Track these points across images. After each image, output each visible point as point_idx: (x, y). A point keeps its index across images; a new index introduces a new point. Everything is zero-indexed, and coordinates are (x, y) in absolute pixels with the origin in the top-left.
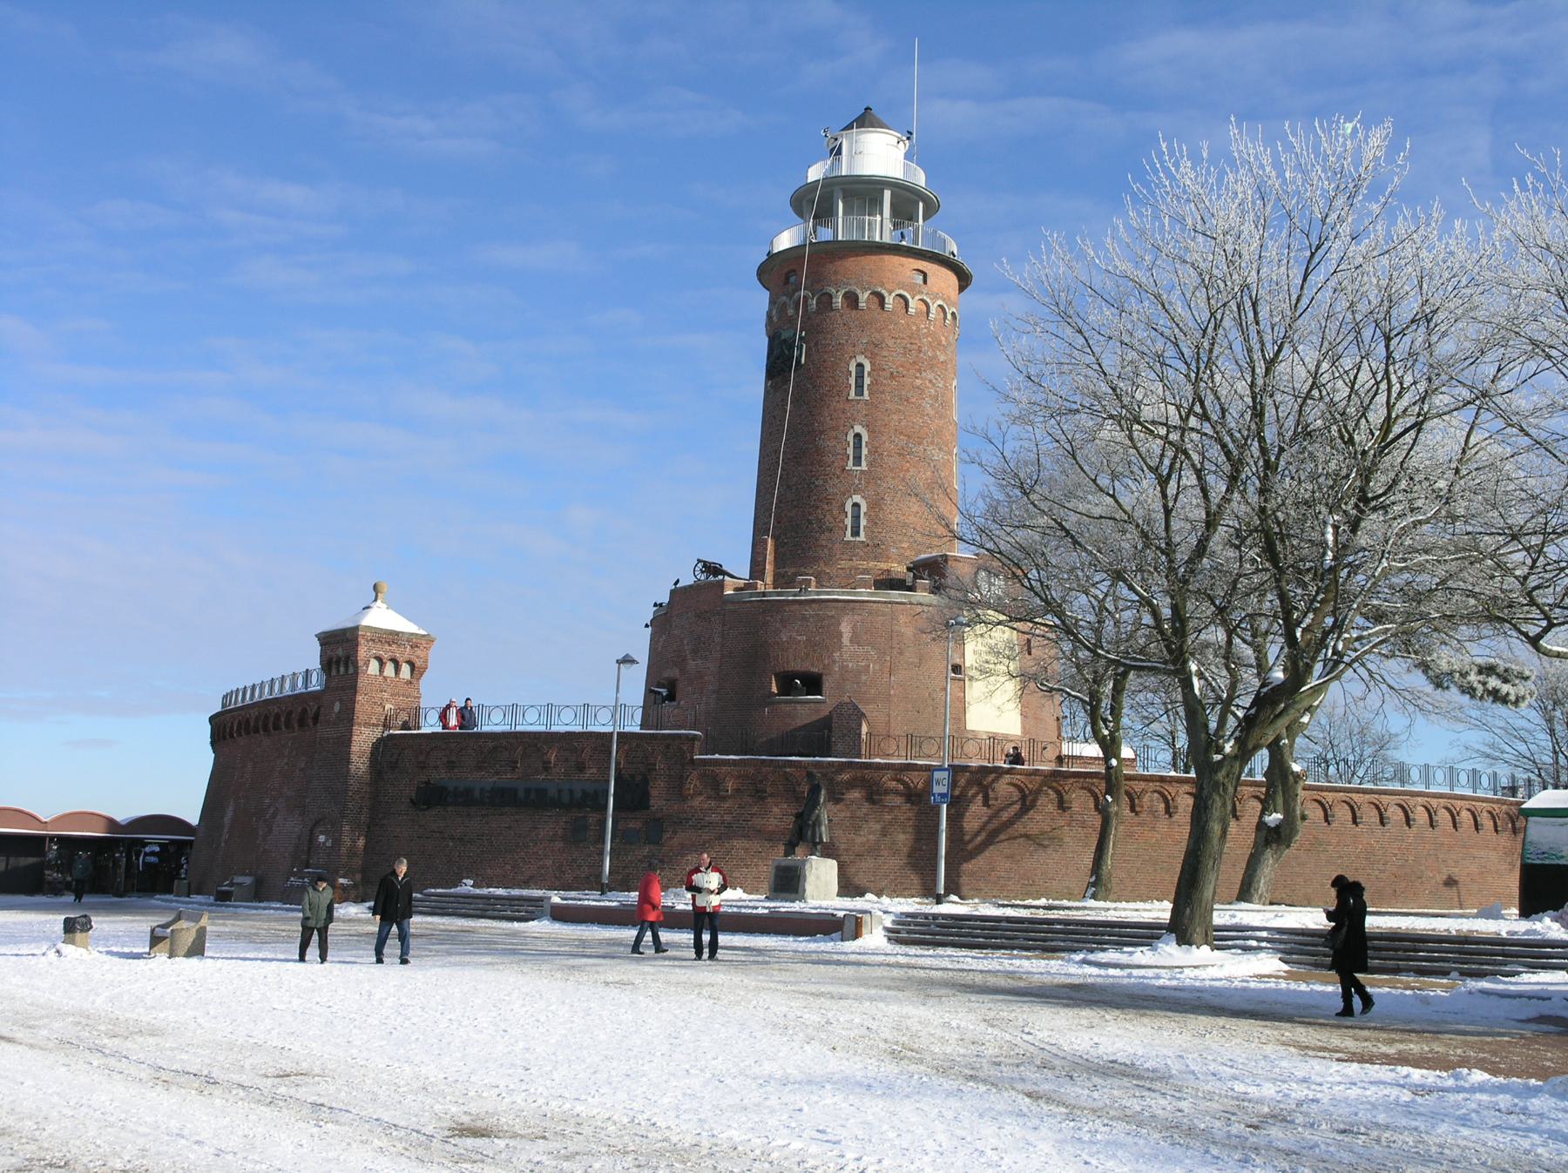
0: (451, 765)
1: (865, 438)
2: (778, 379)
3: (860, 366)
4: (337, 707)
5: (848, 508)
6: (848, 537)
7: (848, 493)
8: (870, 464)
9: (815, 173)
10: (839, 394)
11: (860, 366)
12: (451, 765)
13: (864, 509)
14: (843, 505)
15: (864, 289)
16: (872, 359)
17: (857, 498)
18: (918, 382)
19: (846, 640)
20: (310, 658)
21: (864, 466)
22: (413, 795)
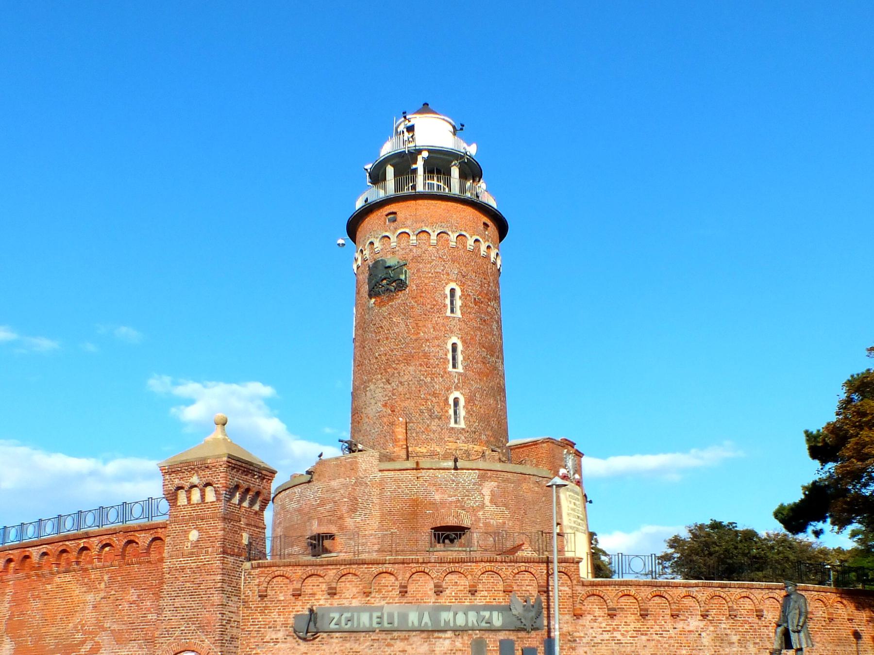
0: (332, 593)
1: (460, 347)
2: (384, 298)
3: (453, 291)
4: (194, 535)
5: (451, 402)
6: (452, 424)
7: (448, 389)
8: (465, 368)
9: (387, 149)
10: (439, 311)
11: (453, 291)
12: (332, 593)
13: (462, 402)
14: (447, 400)
15: (453, 232)
16: (462, 285)
17: (457, 394)
18: (489, 309)
19: (487, 502)
20: (155, 488)
21: (460, 369)
22: (291, 621)
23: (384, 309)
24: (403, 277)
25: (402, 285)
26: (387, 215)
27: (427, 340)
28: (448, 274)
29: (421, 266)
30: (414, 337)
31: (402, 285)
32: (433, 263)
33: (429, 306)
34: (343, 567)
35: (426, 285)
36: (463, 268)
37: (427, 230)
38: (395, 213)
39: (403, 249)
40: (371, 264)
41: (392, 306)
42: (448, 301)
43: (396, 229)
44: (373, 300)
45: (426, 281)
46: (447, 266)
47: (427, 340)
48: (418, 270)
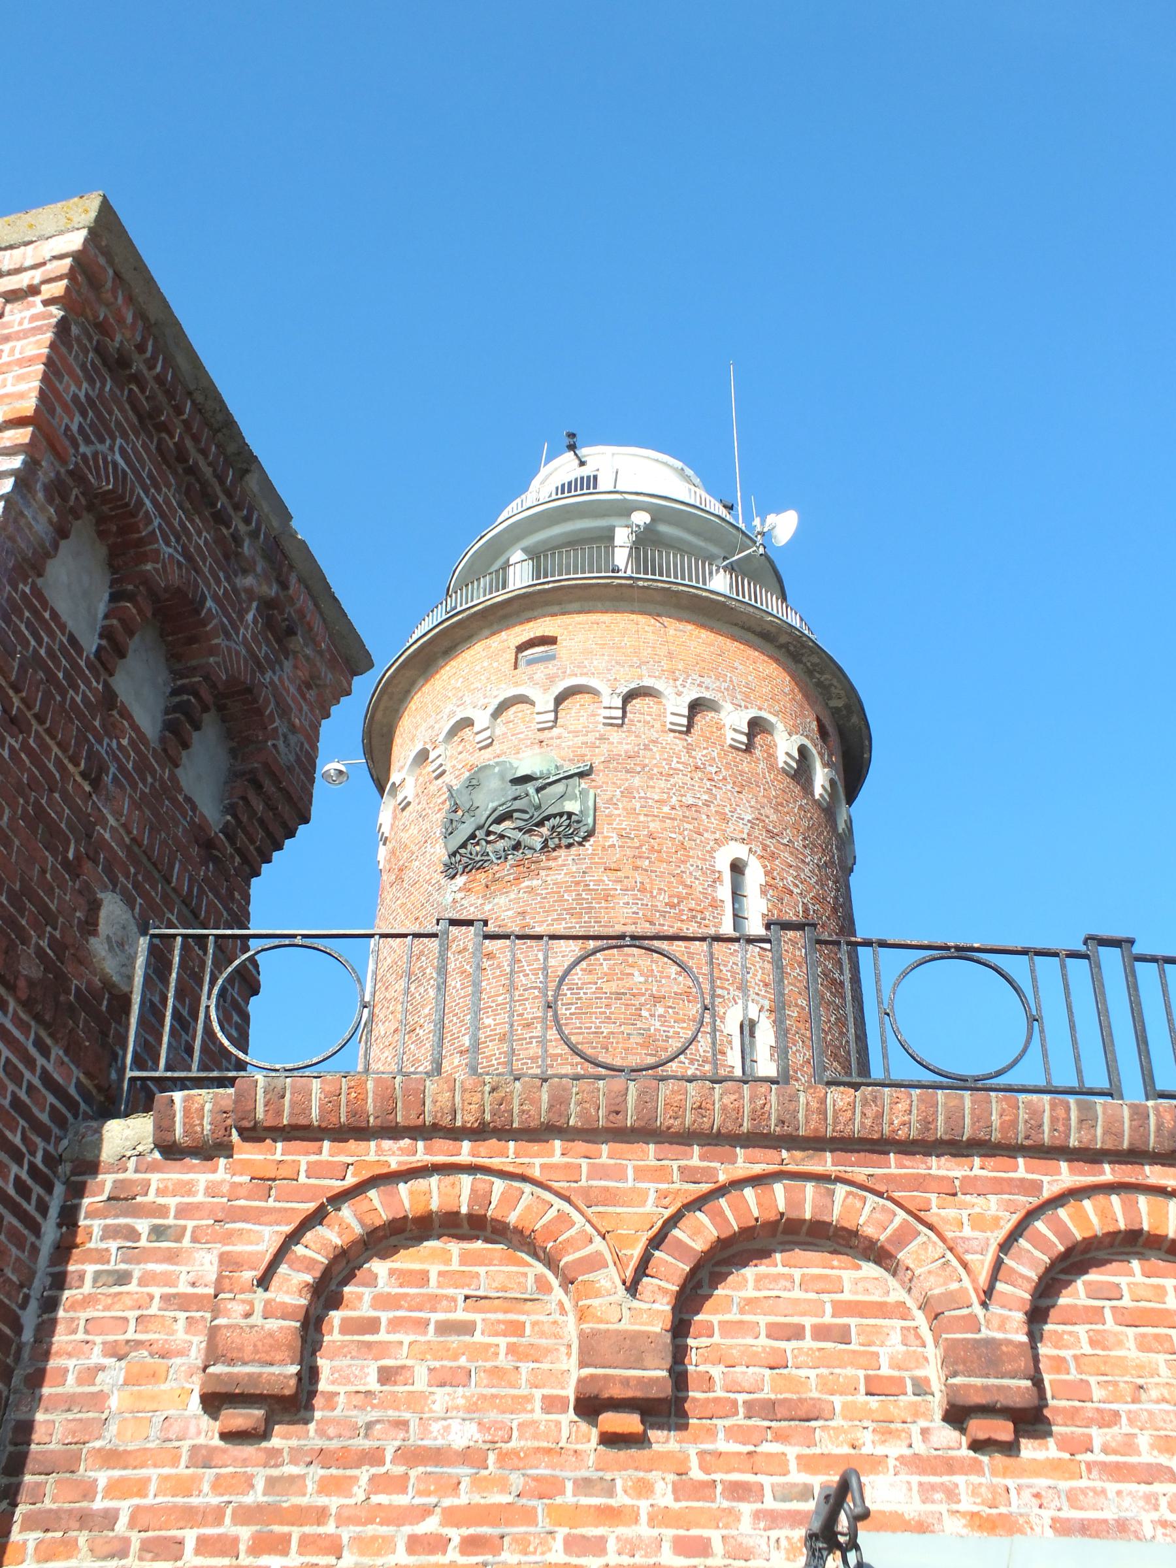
2: (505, 870)
3: (737, 868)
11: (737, 868)
16: (768, 857)
23: (502, 900)
24: (571, 806)
25: (570, 831)
26: (521, 648)
27: (657, 999)
28: (725, 819)
29: (637, 781)
30: (613, 986)
31: (570, 831)
32: (678, 779)
33: (664, 898)
34: (1065, 1176)
35: (651, 836)
36: (768, 811)
37: (659, 685)
38: (550, 641)
39: (576, 733)
40: (456, 784)
41: (531, 890)
42: (724, 892)
43: (552, 679)
44: (460, 880)
45: (654, 826)
46: (719, 794)
47: (657, 999)
48: (628, 793)
